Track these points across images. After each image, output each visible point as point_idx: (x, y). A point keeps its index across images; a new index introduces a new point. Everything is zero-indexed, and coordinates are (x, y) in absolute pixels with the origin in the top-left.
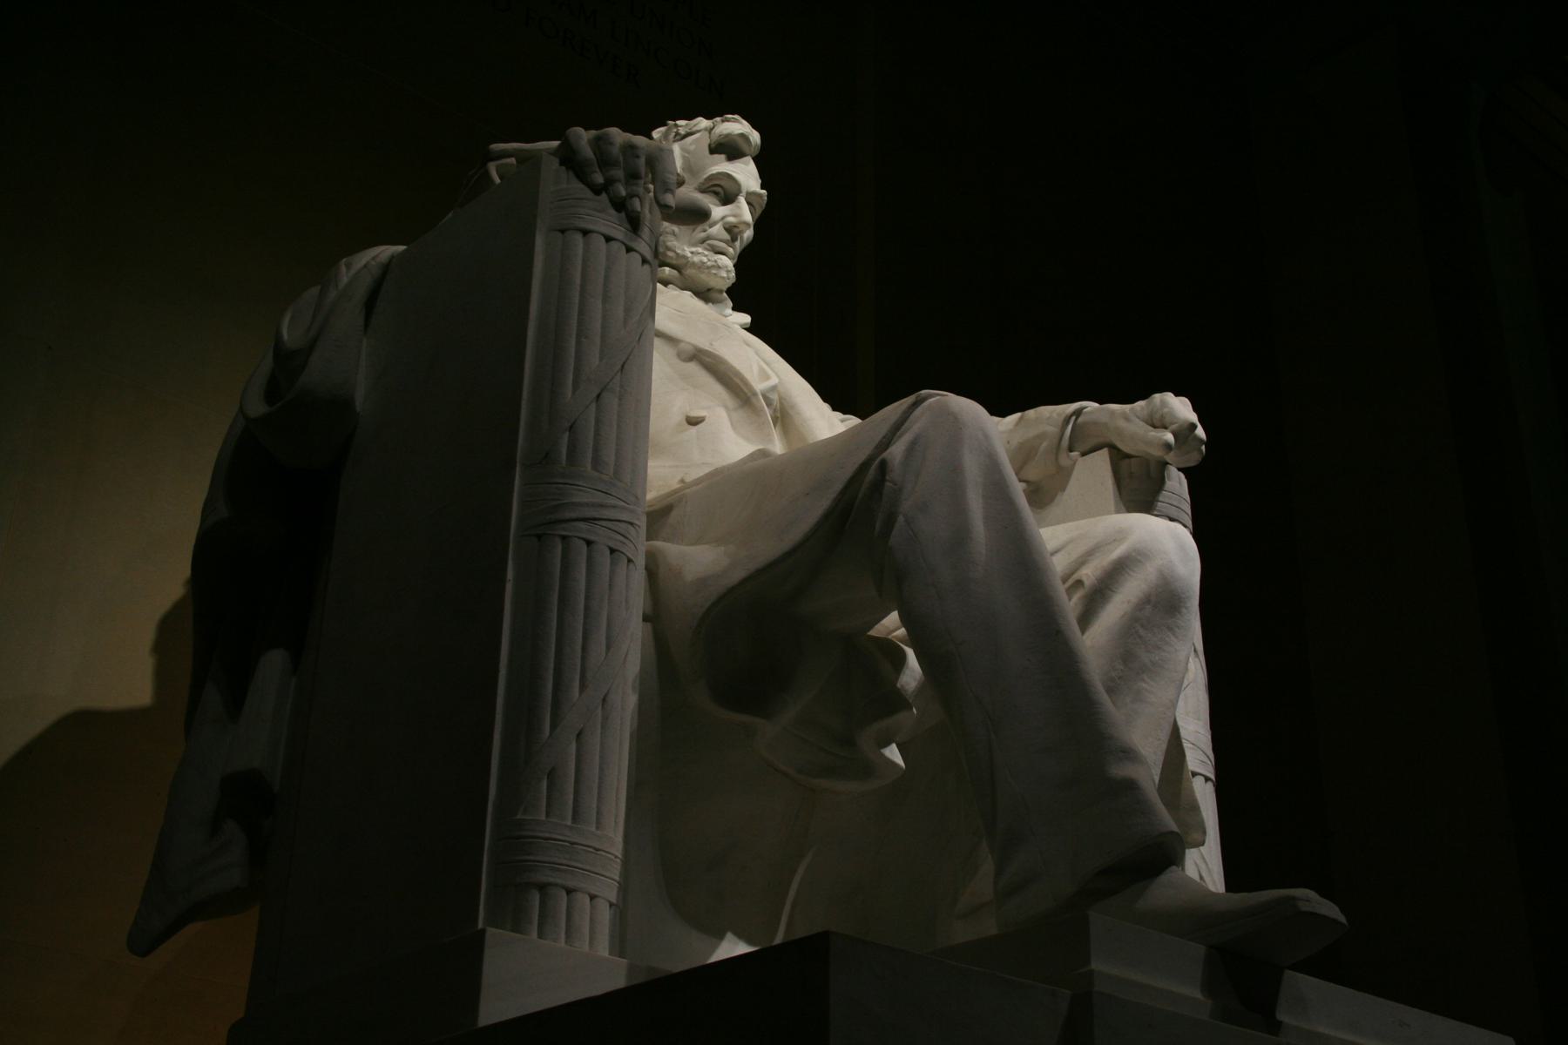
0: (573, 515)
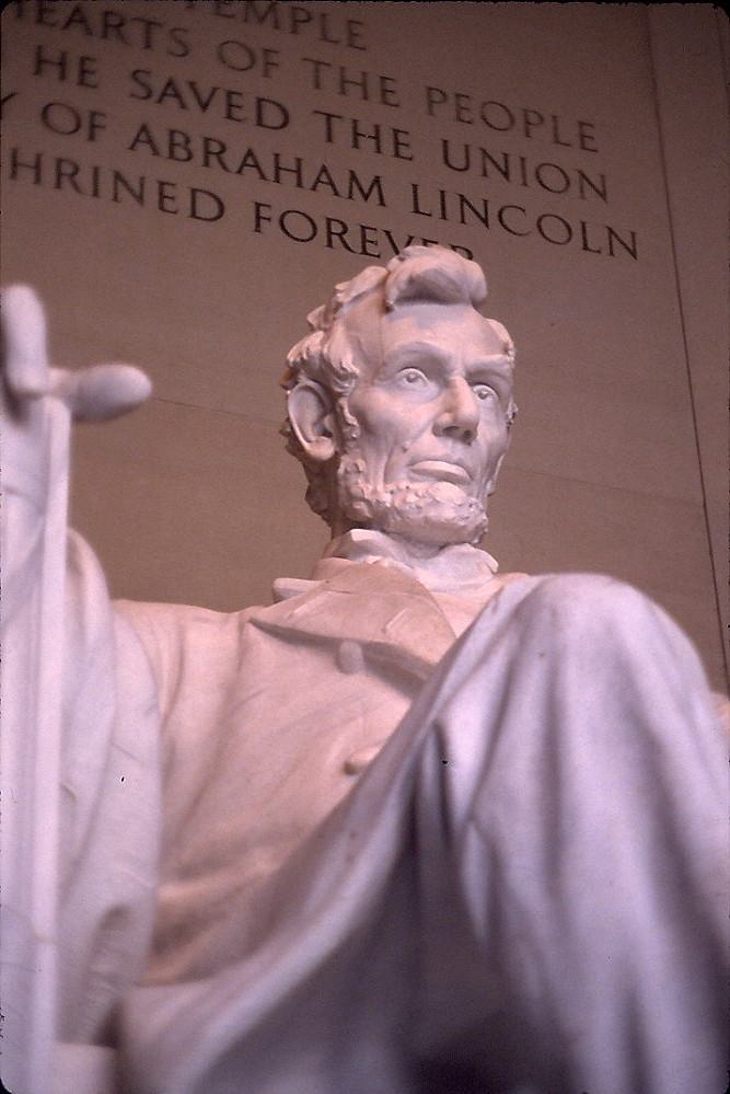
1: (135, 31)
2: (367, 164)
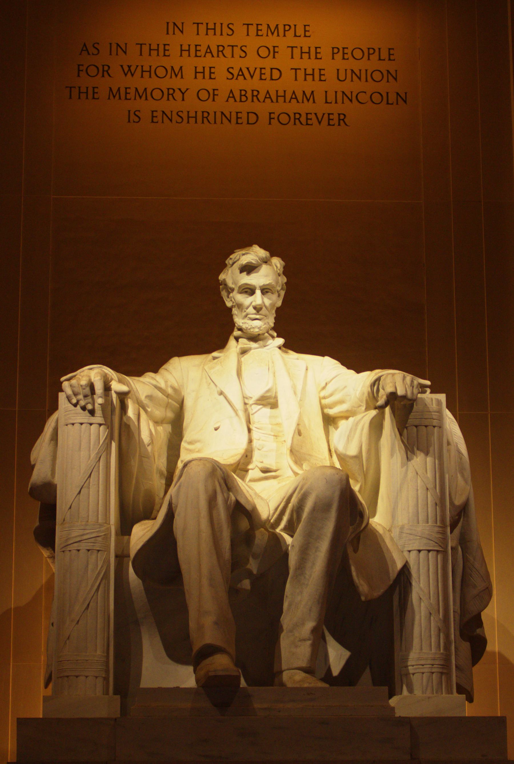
0: (72, 542)
1: (228, 51)
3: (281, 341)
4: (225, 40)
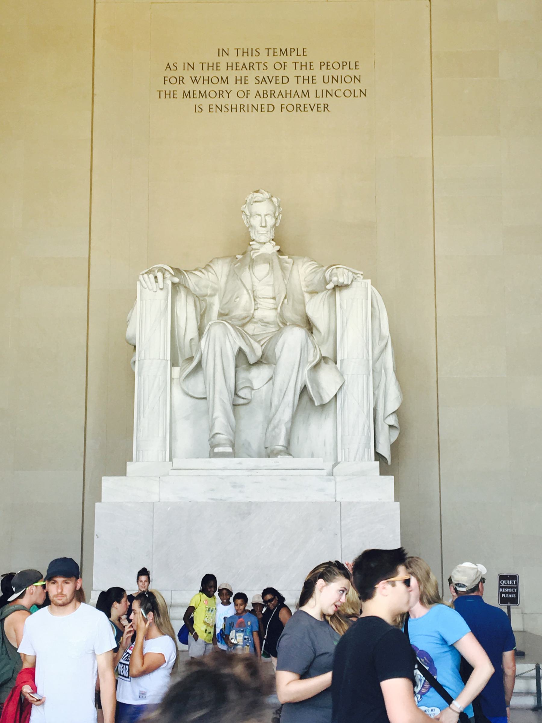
2: (306, 87)
3: (278, 248)
4: (254, 59)
